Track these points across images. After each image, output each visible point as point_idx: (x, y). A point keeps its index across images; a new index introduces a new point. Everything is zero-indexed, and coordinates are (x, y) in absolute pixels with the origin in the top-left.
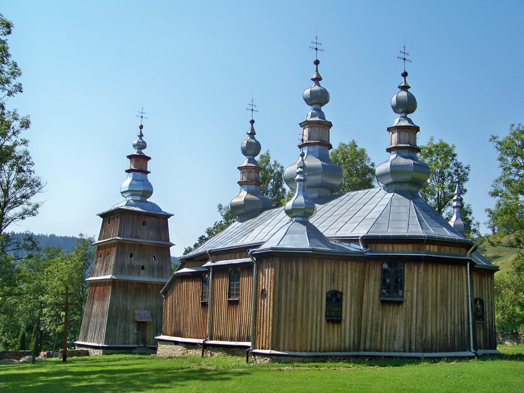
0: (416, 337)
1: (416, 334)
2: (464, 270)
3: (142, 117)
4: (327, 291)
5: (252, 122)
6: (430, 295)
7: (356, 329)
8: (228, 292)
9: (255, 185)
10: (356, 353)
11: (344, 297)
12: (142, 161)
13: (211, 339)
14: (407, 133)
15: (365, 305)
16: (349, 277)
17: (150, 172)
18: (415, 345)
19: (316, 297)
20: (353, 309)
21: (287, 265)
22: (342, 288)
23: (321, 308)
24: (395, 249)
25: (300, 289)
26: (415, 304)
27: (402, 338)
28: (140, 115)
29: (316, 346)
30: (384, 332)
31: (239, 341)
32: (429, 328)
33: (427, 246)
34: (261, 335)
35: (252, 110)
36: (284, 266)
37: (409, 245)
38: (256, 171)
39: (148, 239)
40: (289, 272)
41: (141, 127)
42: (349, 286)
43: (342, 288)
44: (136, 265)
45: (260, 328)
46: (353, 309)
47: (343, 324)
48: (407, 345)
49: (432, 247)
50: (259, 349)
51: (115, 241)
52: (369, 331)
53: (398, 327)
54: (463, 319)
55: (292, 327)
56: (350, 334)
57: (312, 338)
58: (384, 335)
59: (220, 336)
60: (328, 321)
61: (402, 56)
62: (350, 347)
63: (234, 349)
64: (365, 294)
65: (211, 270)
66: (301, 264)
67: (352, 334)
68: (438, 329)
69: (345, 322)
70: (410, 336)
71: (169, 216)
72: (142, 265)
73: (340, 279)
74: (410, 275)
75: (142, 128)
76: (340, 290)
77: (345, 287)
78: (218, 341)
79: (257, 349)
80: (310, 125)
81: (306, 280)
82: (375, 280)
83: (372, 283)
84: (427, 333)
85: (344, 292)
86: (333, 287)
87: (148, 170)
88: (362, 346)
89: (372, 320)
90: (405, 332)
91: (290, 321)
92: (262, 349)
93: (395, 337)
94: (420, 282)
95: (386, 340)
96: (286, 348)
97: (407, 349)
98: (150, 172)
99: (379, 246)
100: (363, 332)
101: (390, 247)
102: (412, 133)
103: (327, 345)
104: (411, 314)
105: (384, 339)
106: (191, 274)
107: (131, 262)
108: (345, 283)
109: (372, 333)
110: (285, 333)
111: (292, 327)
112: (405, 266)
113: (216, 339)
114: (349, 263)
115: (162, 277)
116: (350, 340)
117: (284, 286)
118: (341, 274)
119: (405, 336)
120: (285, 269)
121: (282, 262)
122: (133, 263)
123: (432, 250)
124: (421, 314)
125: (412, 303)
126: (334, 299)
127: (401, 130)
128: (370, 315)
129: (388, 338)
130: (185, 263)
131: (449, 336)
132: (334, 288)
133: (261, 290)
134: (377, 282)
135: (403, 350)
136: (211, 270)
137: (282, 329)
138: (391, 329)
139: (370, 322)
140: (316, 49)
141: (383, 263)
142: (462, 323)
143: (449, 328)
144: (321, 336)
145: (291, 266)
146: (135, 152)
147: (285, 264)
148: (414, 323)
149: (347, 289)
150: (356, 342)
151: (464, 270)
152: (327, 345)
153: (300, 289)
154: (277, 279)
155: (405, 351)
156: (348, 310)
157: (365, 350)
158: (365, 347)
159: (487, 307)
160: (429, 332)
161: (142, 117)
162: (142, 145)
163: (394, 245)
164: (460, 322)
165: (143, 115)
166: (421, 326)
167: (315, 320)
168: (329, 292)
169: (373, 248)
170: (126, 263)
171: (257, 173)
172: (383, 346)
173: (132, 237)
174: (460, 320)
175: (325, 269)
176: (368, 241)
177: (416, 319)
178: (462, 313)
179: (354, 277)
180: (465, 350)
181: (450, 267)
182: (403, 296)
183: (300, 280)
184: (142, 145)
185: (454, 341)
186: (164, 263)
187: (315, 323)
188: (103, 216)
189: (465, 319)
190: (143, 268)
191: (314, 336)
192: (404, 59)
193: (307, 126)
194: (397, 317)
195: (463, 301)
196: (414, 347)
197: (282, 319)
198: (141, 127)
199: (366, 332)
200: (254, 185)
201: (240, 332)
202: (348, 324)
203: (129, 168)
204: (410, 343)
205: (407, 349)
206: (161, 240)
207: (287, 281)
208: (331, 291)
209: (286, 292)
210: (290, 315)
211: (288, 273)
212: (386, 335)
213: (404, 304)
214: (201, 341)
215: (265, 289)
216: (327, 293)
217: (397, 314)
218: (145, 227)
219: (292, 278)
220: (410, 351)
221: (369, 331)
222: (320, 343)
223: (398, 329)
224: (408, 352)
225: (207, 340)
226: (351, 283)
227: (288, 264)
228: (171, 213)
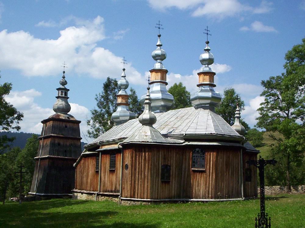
2: (239, 153)
11: (171, 168)
22: (170, 163)
25: (147, 165)
41: (64, 72)
45: (124, 186)
60: (162, 182)
61: (206, 32)
71: (80, 122)
76: (169, 165)
87: (68, 96)
117: (138, 162)
126: (166, 170)
133: (125, 165)
154: (134, 158)
162: (64, 83)
184: (64, 83)
215: (127, 164)
216: (162, 166)
220: (208, 198)
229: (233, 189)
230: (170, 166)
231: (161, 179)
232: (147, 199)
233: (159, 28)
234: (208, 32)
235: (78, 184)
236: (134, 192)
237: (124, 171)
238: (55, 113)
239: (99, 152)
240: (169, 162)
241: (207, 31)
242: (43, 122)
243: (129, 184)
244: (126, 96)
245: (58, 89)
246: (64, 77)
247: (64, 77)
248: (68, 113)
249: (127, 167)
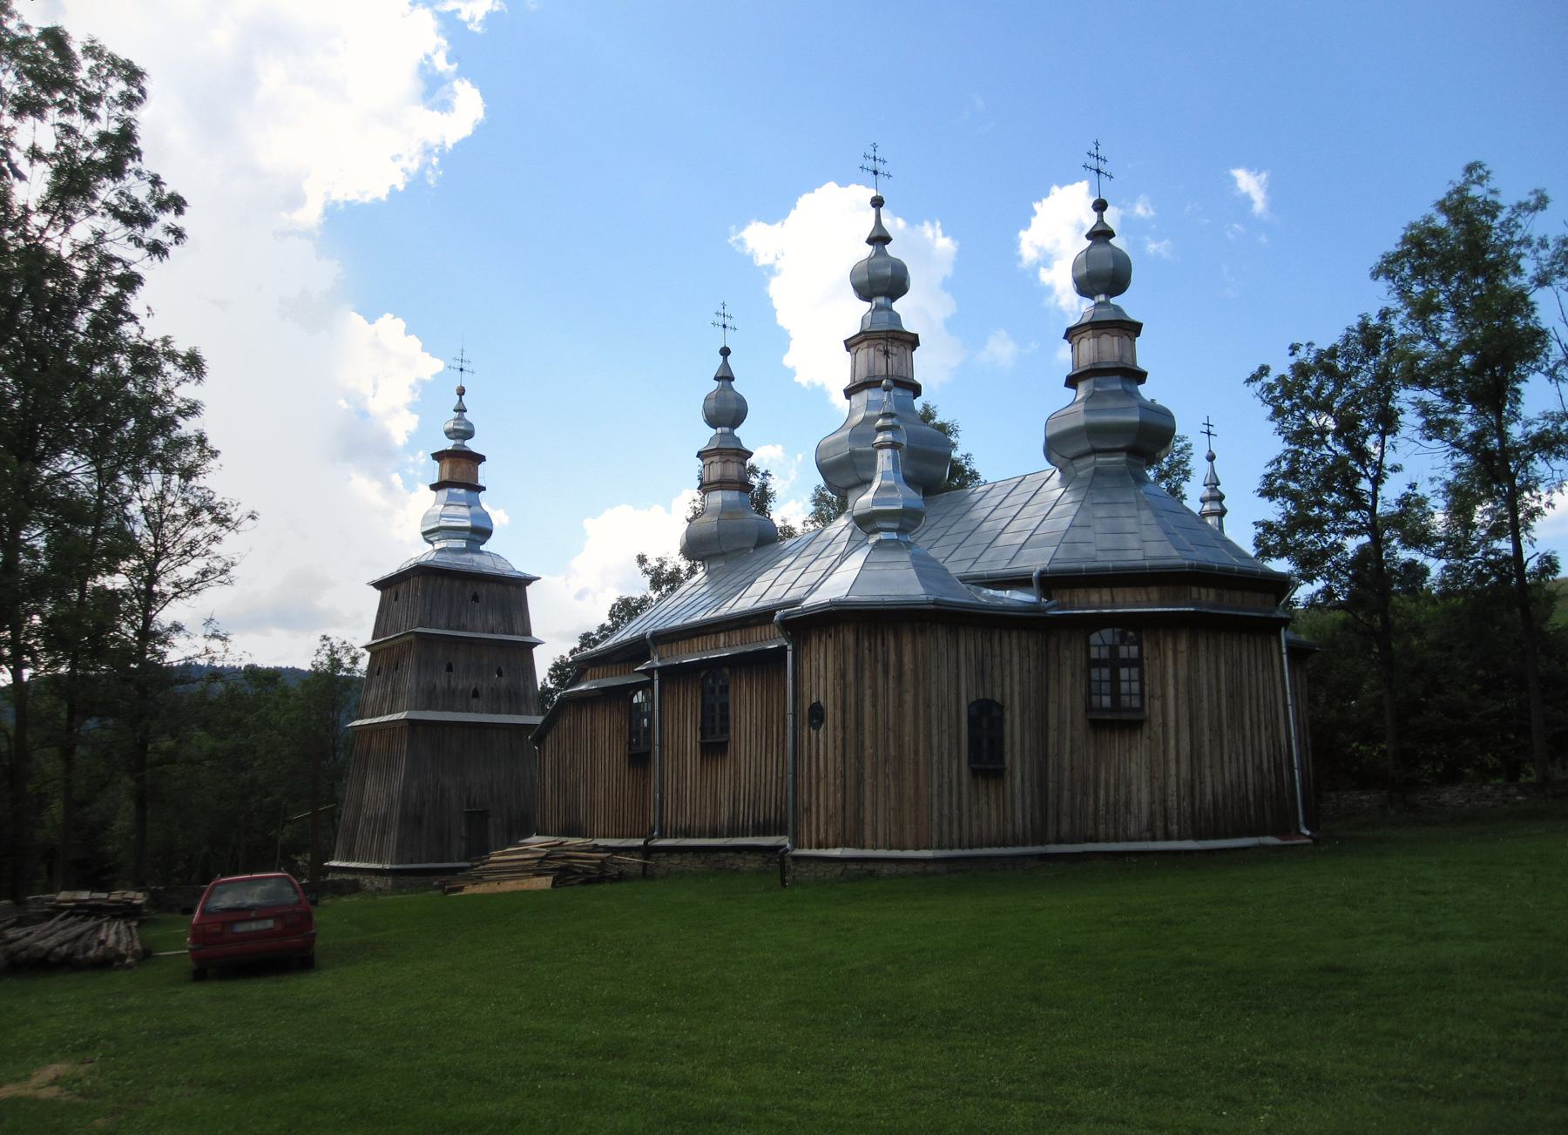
0: (1179, 805)
1: (1178, 796)
2: (1275, 646)
3: (461, 370)
4: (971, 701)
5: (725, 352)
6: (1205, 704)
8: (699, 725)
9: (739, 490)
10: (1038, 849)
11: (1007, 716)
12: (464, 465)
13: (662, 835)
14: (1116, 338)
15: (1052, 735)
16: (1016, 668)
17: (484, 489)
18: (1179, 823)
19: (945, 718)
21: (873, 641)
22: (1003, 694)
23: (959, 743)
24: (1119, 599)
25: (908, 698)
26: (1172, 724)
27: (1145, 806)
28: (458, 365)
29: (950, 833)
30: (1102, 793)
31: (733, 837)
32: (1208, 781)
33: (1195, 590)
34: (814, 816)
35: (724, 326)
36: (866, 644)
37: (1150, 589)
38: (740, 459)
39: (484, 632)
40: (880, 657)
42: (1017, 688)
43: (1003, 694)
44: (460, 687)
46: (1027, 745)
48: (1159, 824)
49: (1203, 591)
50: (810, 848)
51: (412, 637)
52: (1066, 793)
53: (1134, 781)
54: (1278, 758)
55: (892, 790)
56: (1023, 803)
57: (941, 815)
58: (1102, 802)
59: (683, 826)
60: (975, 773)
62: (1024, 834)
63: (723, 855)
64: (1052, 709)
65: (656, 676)
66: (907, 640)
67: (1028, 802)
69: (1012, 773)
70: (1165, 801)
71: (529, 580)
72: (473, 688)
73: (997, 673)
74: (1155, 658)
75: (463, 394)
76: (997, 699)
77: (1007, 690)
78: (678, 840)
79: (803, 848)
80: (871, 342)
81: (921, 677)
82: (1073, 675)
83: (1068, 680)
84: (1203, 794)
86: (981, 694)
87: (481, 482)
88: (1051, 832)
89: (1072, 769)
90: (1152, 793)
91: (887, 775)
92: (819, 846)
93: (1128, 804)
94: (1183, 673)
95: (1107, 812)
96: (880, 842)
97: (1159, 833)
98: (484, 489)
99: (1080, 595)
100: (1051, 798)
101: (1106, 594)
102: (1126, 338)
103: (975, 831)
104: (1165, 752)
105: (1102, 813)
106: (600, 693)
107: (449, 682)
109: (1073, 798)
110: (875, 805)
111: (892, 790)
112: (1144, 636)
113: (673, 835)
115: (519, 713)
116: (1024, 817)
117: (868, 692)
118: (997, 660)
119: (1152, 803)
120: (870, 650)
121: (860, 636)
122: (453, 684)
123: (1204, 598)
124: (1188, 748)
125: (1165, 725)
127: (1101, 331)
128: (1067, 756)
129: (1111, 809)
130: (586, 670)
131: (1251, 799)
132: (984, 695)
134: (1078, 679)
135: (1149, 835)
136: (656, 676)
137: (868, 794)
138: (1117, 788)
139: (1067, 774)
140: (876, 173)
141: (1091, 633)
142: (1278, 769)
144: (960, 808)
145: (883, 645)
146: (449, 444)
147: (869, 640)
148: (1173, 771)
149: (1012, 695)
151: (1275, 646)
152: (975, 831)
153: (908, 698)
154: (851, 676)
155: (1154, 839)
156: (1017, 746)
157: (1059, 841)
158: (1058, 832)
160: (1209, 790)
161: (461, 370)
163: (1114, 590)
164: (1272, 764)
165: (464, 365)
166: (1189, 777)
168: (973, 703)
169: (1066, 599)
170: (438, 684)
171: (742, 463)
172: (1102, 827)
173: (448, 628)
174: (1272, 759)
175: (962, 649)
176: (1050, 582)
177: (1178, 762)
179: (1026, 667)
181: (1244, 637)
182: (1142, 709)
183: (908, 676)
186: (522, 683)
187: (946, 779)
188: (380, 585)
189: (1284, 757)
190: (476, 694)
191: (946, 811)
192: (1098, 171)
193: (865, 344)
194: (1130, 759)
195: (1277, 718)
196: (1175, 827)
197: (868, 770)
199: (1059, 797)
200: (735, 490)
201: (734, 816)
202: (1018, 780)
203: (436, 480)
204: (1166, 818)
205: (1159, 833)
206: (513, 633)
207: (874, 679)
208: (978, 701)
209: (874, 705)
210: (886, 761)
211: (876, 660)
212: (1107, 800)
213: (1146, 726)
214: (640, 842)
215: (819, 702)
216: (969, 707)
217: (1129, 752)
218: (478, 605)
219: (886, 672)
220: (1168, 837)
221: (1066, 793)
222: (960, 827)
223: (1134, 788)
224: (1161, 840)
225: (653, 838)
226: (1021, 682)
227: (876, 639)
228: (537, 575)
230: (1001, 707)
231: (970, 762)
232: (917, 849)
233: (876, 173)
234: (1101, 163)
235: (548, 814)
236: (860, 822)
237: (806, 734)
238: (430, 547)
239: (649, 672)
241: (1098, 159)
242: (380, 585)
243: (832, 788)
244: (737, 455)
245: (438, 456)
246: (461, 410)
248: (482, 548)
249: (817, 714)
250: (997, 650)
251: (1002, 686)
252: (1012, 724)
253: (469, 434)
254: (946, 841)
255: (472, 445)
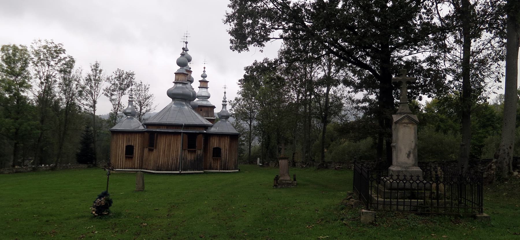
7: (141, 160)
20: (139, 152)
22: (134, 144)
43: (134, 144)
46: (139, 152)
47: (134, 158)
60: (126, 157)
62: (137, 167)
67: (138, 162)
68: (165, 161)
69: (135, 157)
76: (133, 145)
77: (135, 143)
85: (135, 145)
108: (135, 142)
114: (137, 135)
131: (170, 164)
143: (170, 161)
146: (201, 79)
150: (141, 165)
157: (144, 169)
159: (223, 151)
167: (120, 157)
178: (177, 155)
180: (177, 171)
185: (172, 166)
187: (120, 158)
191: (120, 163)
198: (204, 68)
216: (127, 147)
218: (201, 112)
229: (172, 164)
240: (132, 143)
246: (204, 72)
247: (204, 72)
250: (133, 137)
251: (134, 143)
252: (136, 149)
253: (206, 77)
254: (119, 167)
255: (207, 79)
